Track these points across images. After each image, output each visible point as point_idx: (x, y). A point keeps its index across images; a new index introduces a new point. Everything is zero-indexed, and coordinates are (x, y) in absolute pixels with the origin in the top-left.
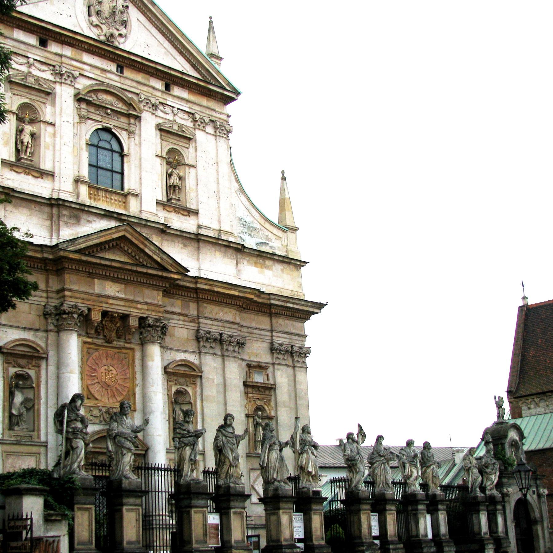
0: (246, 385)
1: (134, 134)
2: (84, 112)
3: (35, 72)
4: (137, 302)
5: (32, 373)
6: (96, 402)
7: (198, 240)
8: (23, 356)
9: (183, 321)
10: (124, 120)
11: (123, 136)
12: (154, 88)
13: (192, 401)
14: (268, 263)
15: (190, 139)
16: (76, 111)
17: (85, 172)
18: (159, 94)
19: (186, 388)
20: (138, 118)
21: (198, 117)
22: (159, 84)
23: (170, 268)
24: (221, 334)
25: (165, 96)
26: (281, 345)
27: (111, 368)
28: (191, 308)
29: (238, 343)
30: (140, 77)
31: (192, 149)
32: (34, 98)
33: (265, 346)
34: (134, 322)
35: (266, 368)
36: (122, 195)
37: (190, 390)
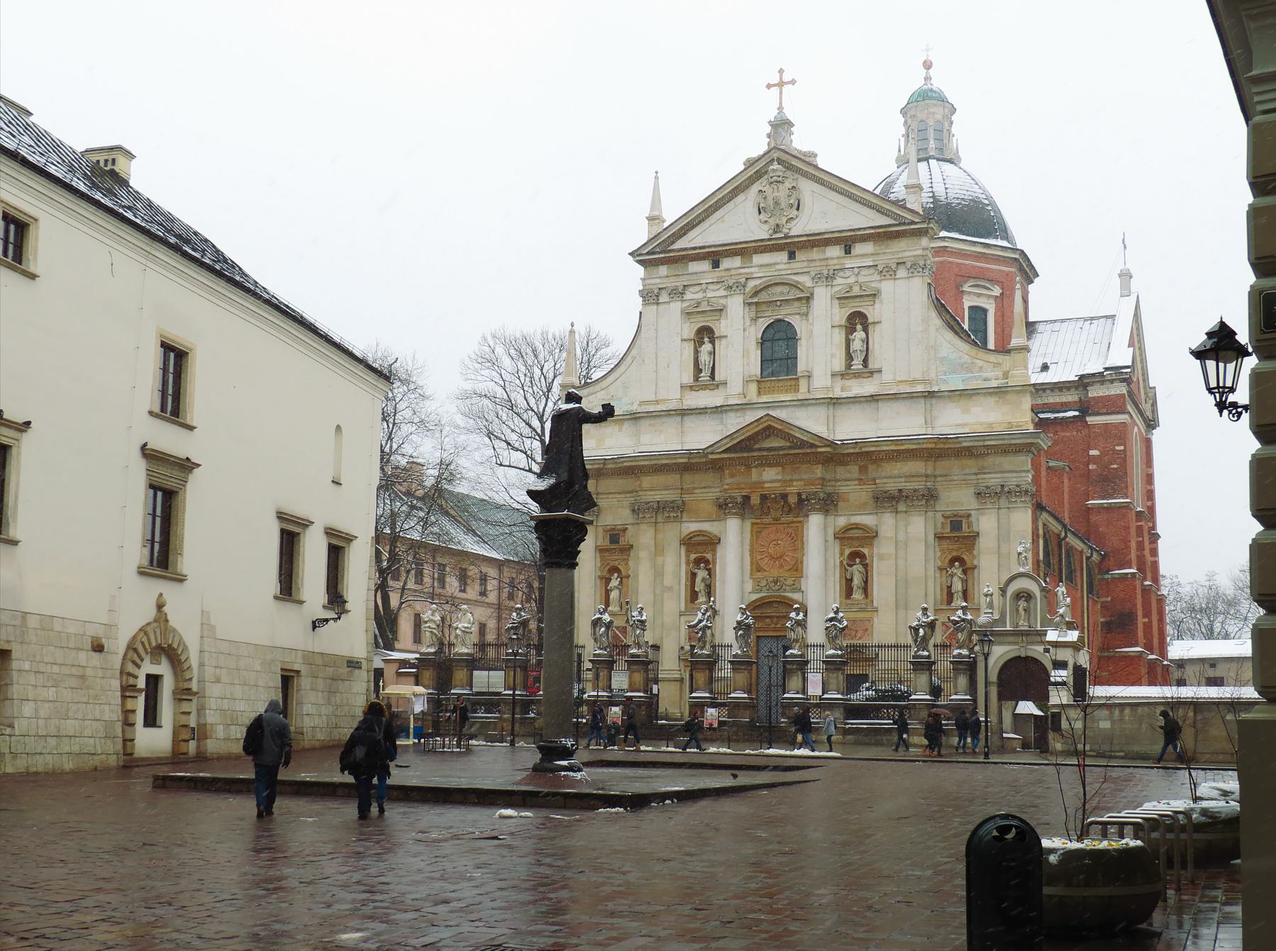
0: (939, 538)
1: (807, 315)
2: (753, 315)
3: (710, 294)
4: (792, 480)
5: (709, 556)
6: (765, 573)
7: (877, 400)
8: (699, 544)
9: (860, 485)
10: (796, 304)
11: (796, 321)
12: (827, 259)
13: (867, 561)
14: (974, 398)
15: (875, 295)
16: (747, 316)
17: (756, 369)
18: (835, 261)
19: (862, 550)
20: (808, 299)
21: (880, 268)
22: (835, 252)
23: (817, 443)
24: (900, 490)
25: (842, 261)
26: (987, 487)
27: (779, 542)
28: (870, 471)
29: (923, 495)
30: (815, 254)
31: (877, 306)
32: (708, 318)
33: (972, 490)
34: (793, 500)
35: (969, 516)
36: (795, 379)
37: (866, 551)
